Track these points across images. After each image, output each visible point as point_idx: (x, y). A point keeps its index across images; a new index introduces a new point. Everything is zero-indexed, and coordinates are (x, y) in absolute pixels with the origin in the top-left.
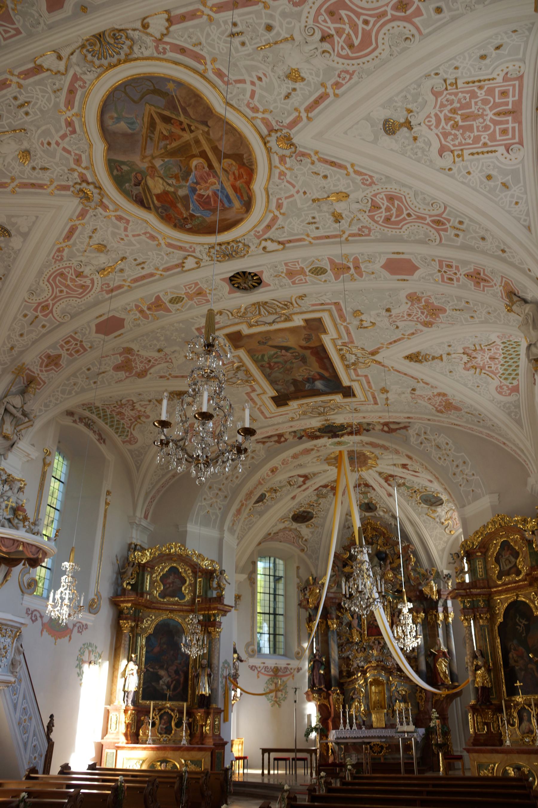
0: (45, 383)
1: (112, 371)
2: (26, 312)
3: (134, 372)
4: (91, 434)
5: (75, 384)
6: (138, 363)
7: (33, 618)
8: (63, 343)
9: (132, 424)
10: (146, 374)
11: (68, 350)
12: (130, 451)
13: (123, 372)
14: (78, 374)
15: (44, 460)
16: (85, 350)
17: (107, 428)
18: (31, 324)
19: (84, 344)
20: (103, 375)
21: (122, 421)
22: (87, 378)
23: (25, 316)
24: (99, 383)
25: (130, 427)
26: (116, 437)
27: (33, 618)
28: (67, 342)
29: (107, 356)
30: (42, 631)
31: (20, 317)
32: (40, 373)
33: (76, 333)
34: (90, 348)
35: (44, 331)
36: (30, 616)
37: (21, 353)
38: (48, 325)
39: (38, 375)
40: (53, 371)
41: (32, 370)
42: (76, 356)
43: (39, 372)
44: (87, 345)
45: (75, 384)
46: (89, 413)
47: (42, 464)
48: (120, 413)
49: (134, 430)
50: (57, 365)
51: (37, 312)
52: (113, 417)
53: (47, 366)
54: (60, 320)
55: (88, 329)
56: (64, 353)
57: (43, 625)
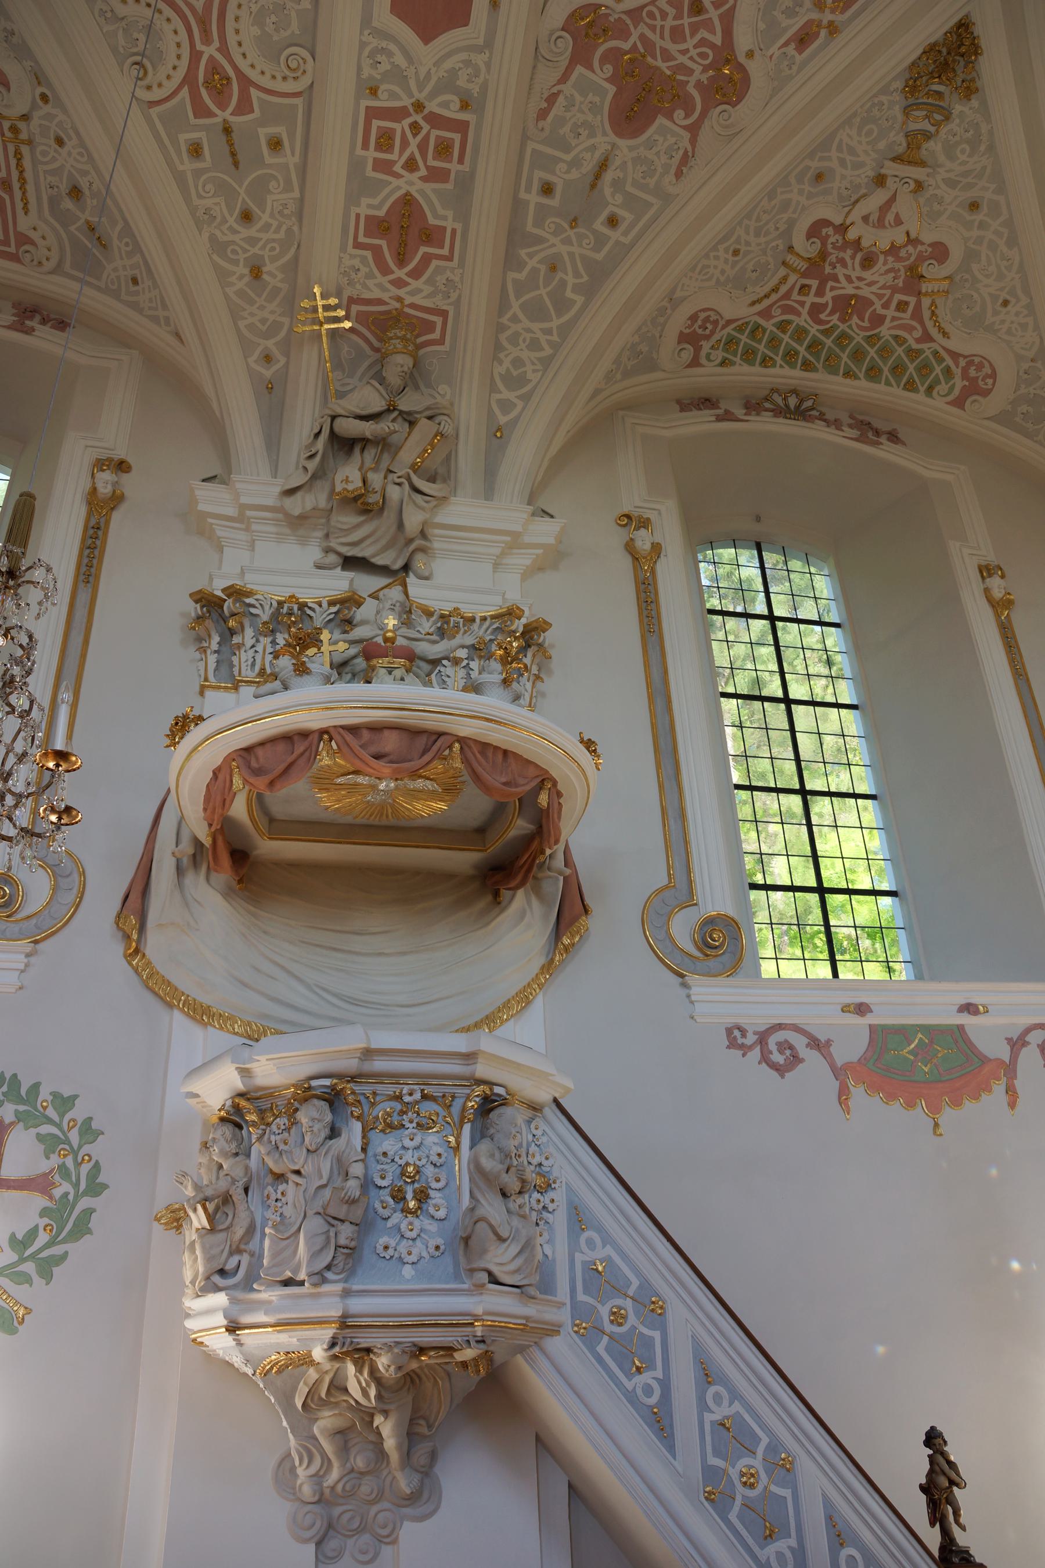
0: (444, 314)
1: (623, 143)
2: (183, 137)
3: (691, 89)
4: (817, 432)
5: (553, 269)
6: (673, 48)
7: (778, 1058)
8: (372, 154)
9: (917, 315)
10: (741, 68)
11: (411, 165)
12: (1003, 418)
13: (661, 120)
14: (530, 227)
15: (630, 547)
16: (462, 127)
17: (861, 389)
18: (236, 164)
19: (432, 107)
20: (609, 176)
21: (885, 331)
22: (574, 223)
23: (196, 150)
24: (621, 212)
25: (927, 338)
26: (917, 402)
27: (778, 1058)
28: (385, 142)
29: (552, 99)
30: (843, 1093)
31: (188, 165)
32: (401, 292)
33: (374, 92)
34: (465, 106)
35: (291, 158)
36: (756, 1053)
37: (293, 267)
38: (281, 130)
39: (399, 299)
40: (435, 263)
41: (366, 295)
42: (454, 166)
43: (394, 291)
44: (445, 105)
45: (553, 269)
46: (757, 369)
47: (627, 562)
48: (845, 305)
49: (945, 335)
50: (431, 236)
51: (211, 114)
52: (843, 335)
53: (401, 260)
54: (290, 87)
55: (392, 47)
56: (411, 184)
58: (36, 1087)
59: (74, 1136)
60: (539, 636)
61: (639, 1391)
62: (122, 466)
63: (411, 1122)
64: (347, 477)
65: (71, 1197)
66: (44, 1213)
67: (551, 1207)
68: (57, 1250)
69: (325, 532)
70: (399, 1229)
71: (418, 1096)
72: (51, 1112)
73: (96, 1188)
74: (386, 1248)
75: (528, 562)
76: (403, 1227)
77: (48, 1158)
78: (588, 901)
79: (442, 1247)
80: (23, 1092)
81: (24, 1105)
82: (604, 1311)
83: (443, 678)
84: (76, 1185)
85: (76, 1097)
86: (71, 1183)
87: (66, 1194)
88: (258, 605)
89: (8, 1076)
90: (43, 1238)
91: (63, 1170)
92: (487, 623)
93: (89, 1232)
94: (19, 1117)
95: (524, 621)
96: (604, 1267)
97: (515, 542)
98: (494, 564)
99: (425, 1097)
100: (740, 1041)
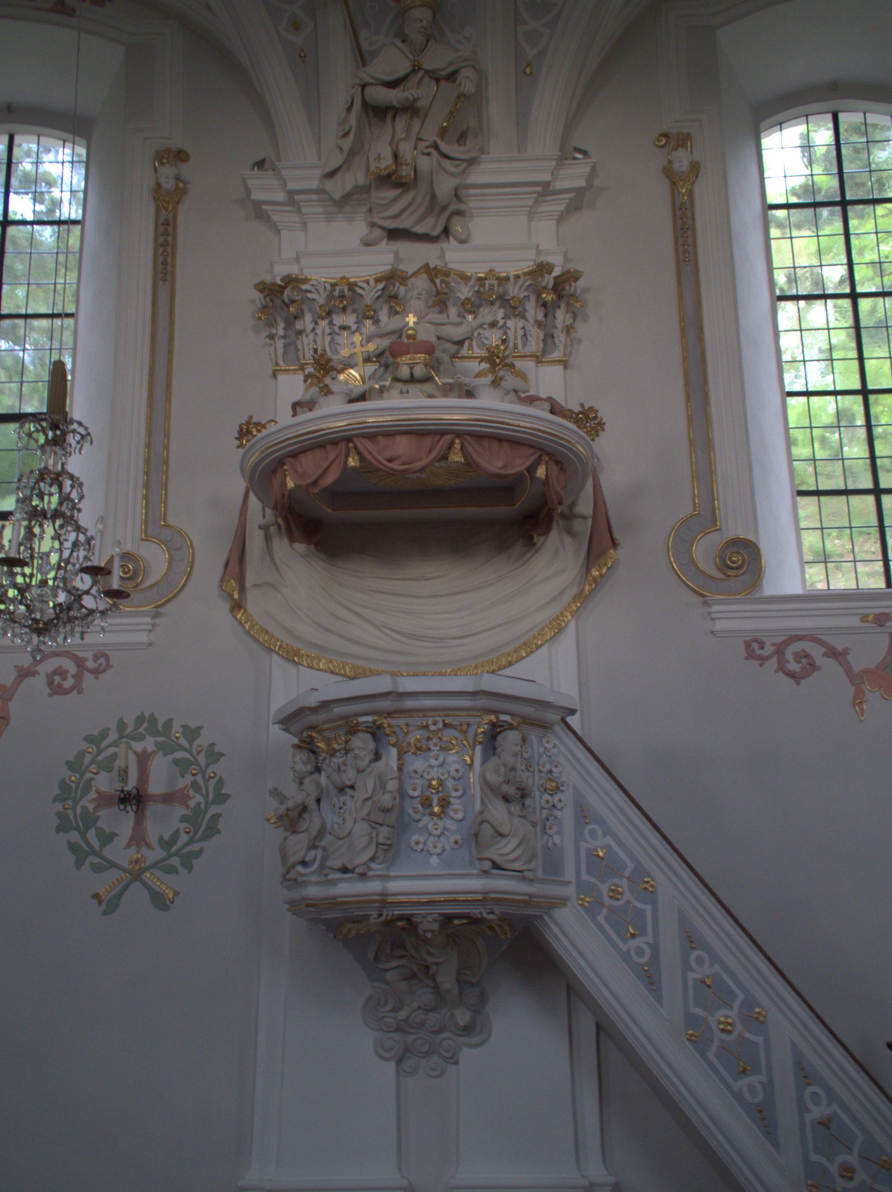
7: (794, 666)
57: (855, 678)
58: (169, 724)
59: (202, 759)
60: (570, 286)
61: (633, 953)
62: (181, 156)
63: (435, 745)
64: (379, 155)
65: (203, 806)
66: (184, 819)
67: (559, 805)
68: (195, 847)
69: (368, 206)
70: (427, 829)
71: (440, 725)
72: (183, 742)
73: (221, 798)
74: (417, 843)
75: (562, 207)
76: (430, 826)
77: (183, 776)
78: (616, 535)
79: (460, 842)
80: (160, 727)
81: (162, 736)
82: (604, 889)
83: (483, 339)
84: (206, 797)
85: (201, 728)
86: (202, 795)
87: (199, 804)
88: (313, 290)
89: (147, 715)
90: (184, 838)
91: (195, 785)
92: (521, 281)
93: (219, 832)
94: (160, 747)
95: (554, 274)
96: (605, 854)
97: (546, 191)
98: (530, 213)
99: (446, 725)
100: (758, 652)
